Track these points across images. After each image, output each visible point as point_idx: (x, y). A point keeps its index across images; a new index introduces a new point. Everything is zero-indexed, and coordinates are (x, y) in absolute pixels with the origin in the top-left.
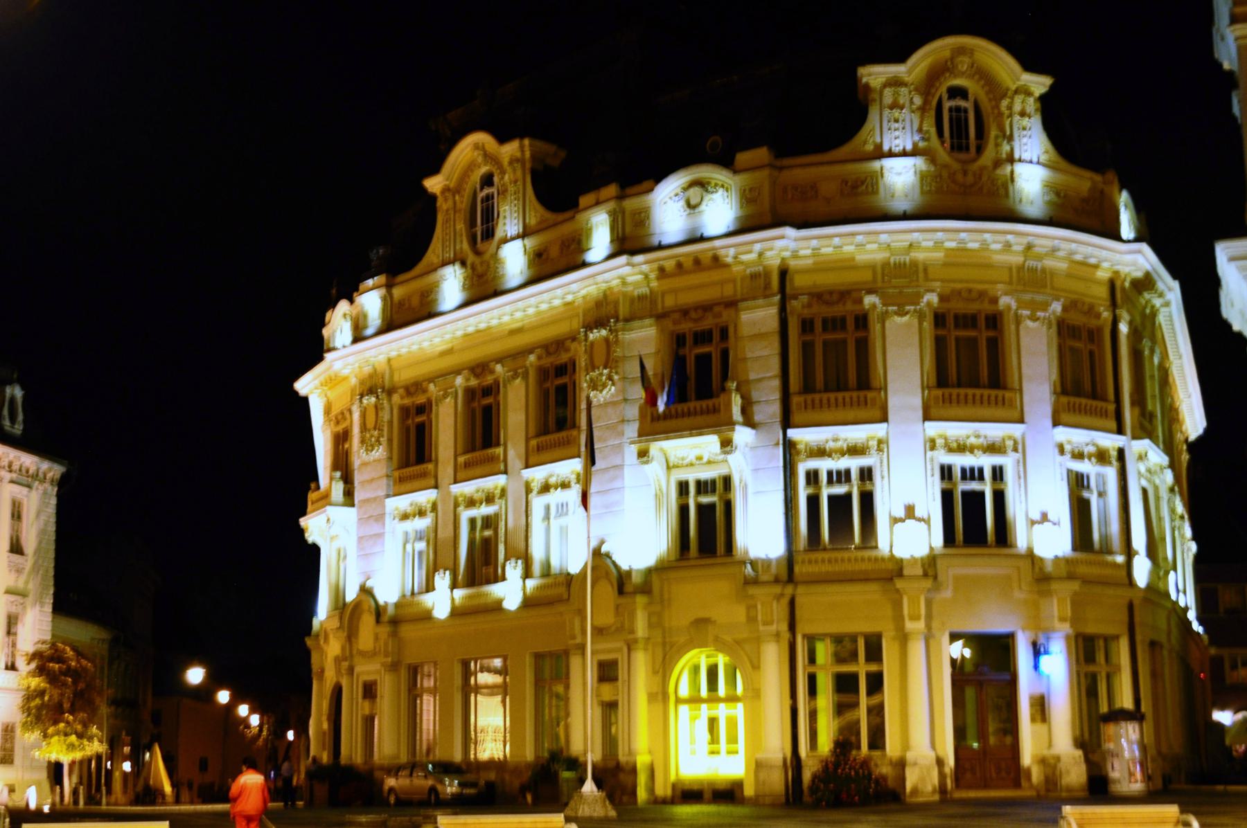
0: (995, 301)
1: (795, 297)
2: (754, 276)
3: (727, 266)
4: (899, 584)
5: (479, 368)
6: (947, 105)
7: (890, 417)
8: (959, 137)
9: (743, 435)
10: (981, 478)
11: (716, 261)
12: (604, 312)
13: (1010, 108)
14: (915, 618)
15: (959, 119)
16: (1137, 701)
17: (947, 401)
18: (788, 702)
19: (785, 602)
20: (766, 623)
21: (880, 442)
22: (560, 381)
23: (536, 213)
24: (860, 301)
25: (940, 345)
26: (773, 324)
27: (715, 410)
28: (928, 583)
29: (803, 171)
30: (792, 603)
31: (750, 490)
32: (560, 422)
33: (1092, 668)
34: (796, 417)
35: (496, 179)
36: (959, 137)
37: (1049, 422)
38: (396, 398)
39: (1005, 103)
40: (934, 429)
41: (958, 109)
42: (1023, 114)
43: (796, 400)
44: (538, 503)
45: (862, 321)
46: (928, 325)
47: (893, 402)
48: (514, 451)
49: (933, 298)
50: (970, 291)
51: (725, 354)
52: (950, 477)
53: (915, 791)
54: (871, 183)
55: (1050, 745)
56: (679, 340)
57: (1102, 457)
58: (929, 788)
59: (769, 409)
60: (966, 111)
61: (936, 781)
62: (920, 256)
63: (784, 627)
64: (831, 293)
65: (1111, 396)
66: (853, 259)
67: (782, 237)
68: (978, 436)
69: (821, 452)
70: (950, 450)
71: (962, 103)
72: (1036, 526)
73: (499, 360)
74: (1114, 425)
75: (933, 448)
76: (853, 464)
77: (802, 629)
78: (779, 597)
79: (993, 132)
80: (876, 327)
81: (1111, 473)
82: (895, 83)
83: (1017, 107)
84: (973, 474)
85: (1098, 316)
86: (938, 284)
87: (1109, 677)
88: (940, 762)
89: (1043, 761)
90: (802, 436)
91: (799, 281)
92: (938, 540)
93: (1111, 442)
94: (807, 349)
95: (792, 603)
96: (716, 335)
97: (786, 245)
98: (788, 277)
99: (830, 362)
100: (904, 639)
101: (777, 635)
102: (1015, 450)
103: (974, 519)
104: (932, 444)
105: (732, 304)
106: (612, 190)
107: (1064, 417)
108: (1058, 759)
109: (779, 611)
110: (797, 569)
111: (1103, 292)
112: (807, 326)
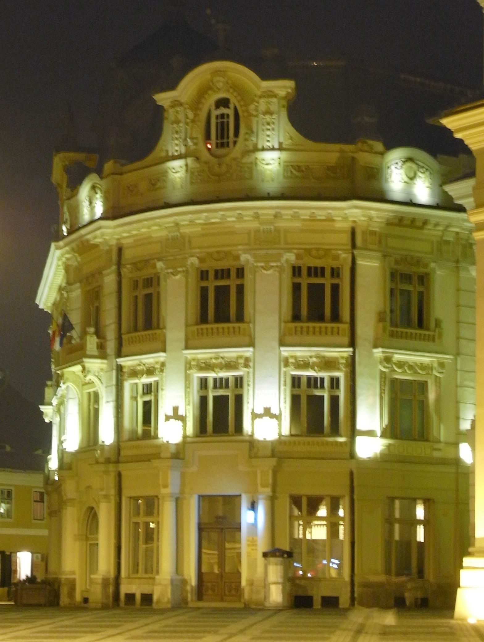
0: (237, 258)
7: (168, 348)
8: (222, 137)
17: (200, 333)
29: (135, 175)
34: (124, 350)
36: (222, 137)
37: (276, 344)
41: (222, 116)
49: (194, 261)
50: (218, 252)
53: (158, 601)
54: (158, 181)
57: (328, 364)
58: (166, 600)
60: (228, 116)
67: (100, 228)
68: (216, 358)
72: (257, 421)
74: (346, 340)
75: (190, 368)
78: (106, 472)
79: (242, 130)
80: (162, 283)
86: (197, 250)
90: (127, 362)
92: (190, 430)
93: (342, 353)
95: (119, 475)
98: (123, 251)
102: (246, 366)
103: (220, 415)
104: (188, 366)
107: (288, 339)
109: (111, 480)
111: (346, 239)
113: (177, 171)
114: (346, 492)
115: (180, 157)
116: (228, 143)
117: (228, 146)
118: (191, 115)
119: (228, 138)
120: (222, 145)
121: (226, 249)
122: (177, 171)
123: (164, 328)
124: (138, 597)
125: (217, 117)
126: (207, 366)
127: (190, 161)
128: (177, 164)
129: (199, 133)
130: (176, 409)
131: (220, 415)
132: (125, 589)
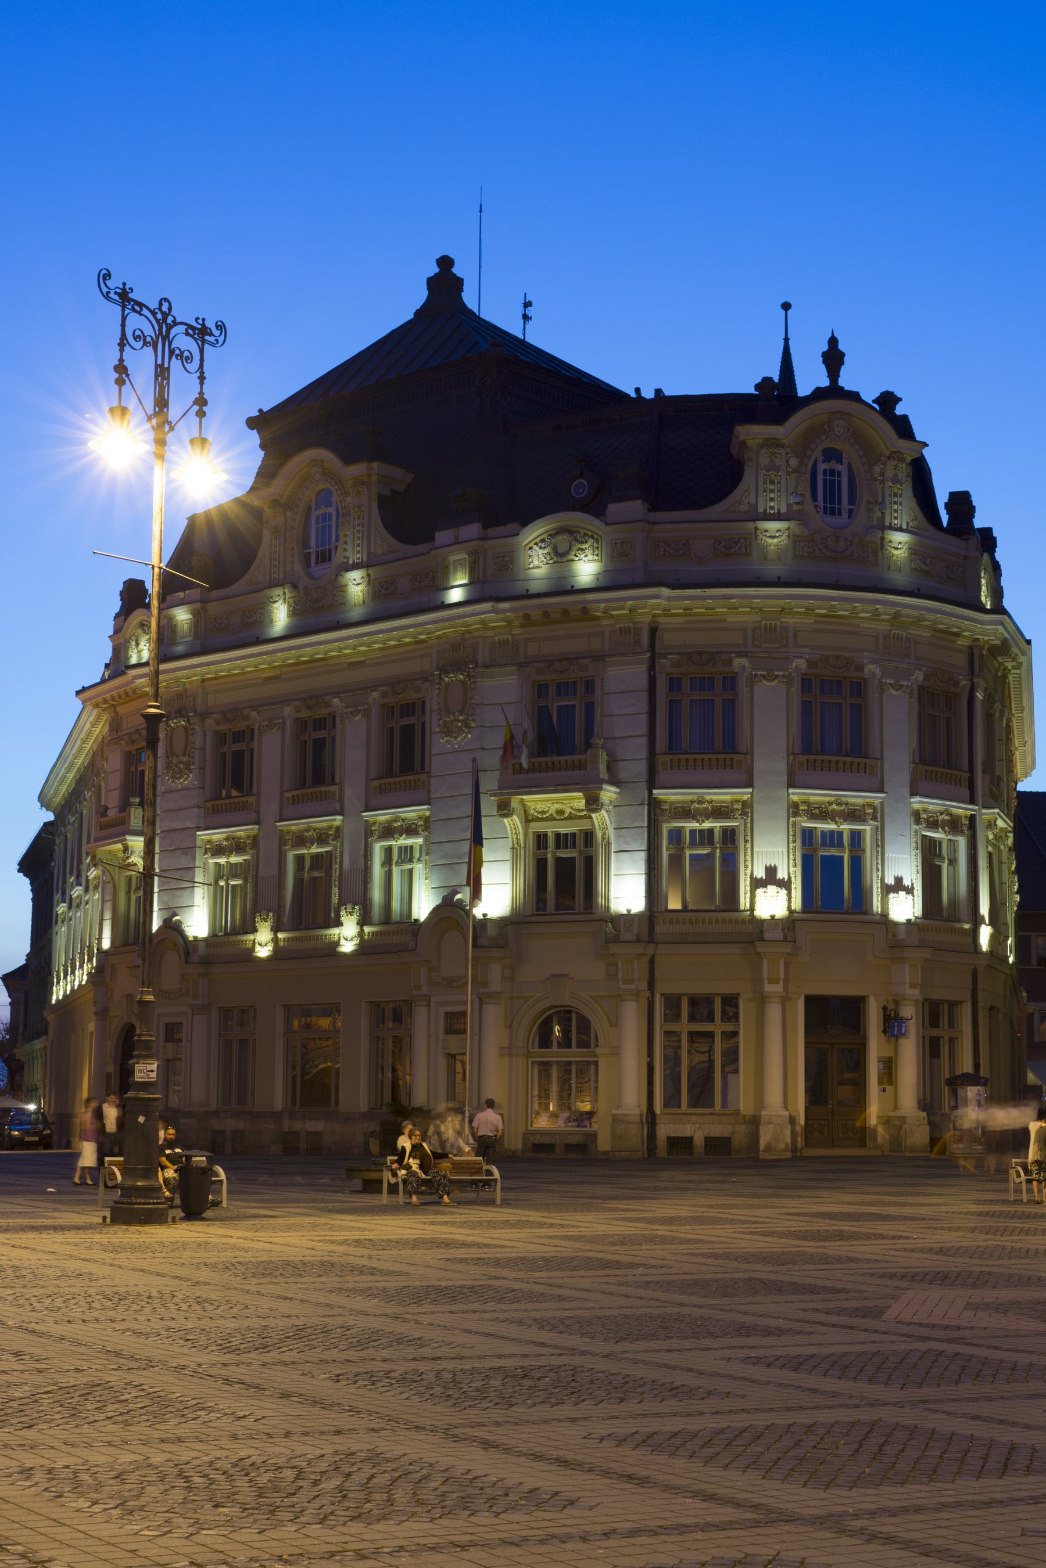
0: (860, 668)
1: (664, 655)
2: (622, 631)
3: (597, 618)
4: (761, 947)
5: (311, 700)
6: (822, 467)
7: (756, 782)
8: (832, 502)
9: (609, 793)
10: (841, 845)
11: (586, 613)
12: (460, 657)
13: (882, 474)
14: (774, 981)
15: (832, 482)
16: (977, 1066)
18: (645, 1060)
19: (647, 958)
20: (625, 982)
21: (744, 804)
22: (407, 721)
23: (383, 542)
24: (730, 663)
25: (806, 707)
26: (642, 682)
27: (581, 766)
28: (787, 948)
30: (652, 962)
31: (613, 848)
32: (404, 763)
33: (936, 1033)
34: (661, 777)
35: (334, 499)
37: (907, 791)
38: (210, 723)
39: (877, 469)
40: (796, 795)
41: (832, 472)
42: (895, 480)
43: (661, 759)
44: (378, 849)
45: (730, 682)
46: (796, 689)
47: (759, 766)
48: (352, 792)
49: (802, 664)
50: (838, 657)
51: (590, 708)
52: (811, 843)
53: (768, 1149)
54: (747, 543)
55: (895, 1108)
56: (541, 689)
58: (782, 1146)
59: (636, 767)
60: (839, 473)
61: (789, 1140)
62: (790, 620)
63: (644, 985)
64: (701, 653)
65: (966, 767)
66: (724, 621)
67: (657, 597)
68: (839, 804)
69: (685, 812)
70: (813, 817)
71: (838, 467)
73: (336, 694)
75: (796, 814)
76: (715, 825)
77: (661, 988)
81: (962, 842)
82: (773, 443)
83: (890, 474)
84: (833, 839)
85: (957, 684)
86: (807, 650)
87: (952, 1040)
88: (792, 1120)
89: (887, 1121)
91: (668, 639)
93: (961, 810)
94: (673, 707)
95: (652, 962)
96: (581, 688)
97: (658, 602)
98: (657, 634)
99: (697, 726)
100: (762, 1000)
101: (637, 994)
102: (874, 818)
103: (834, 882)
104: (794, 809)
105: (599, 657)
106: (473, 529)
108: (903, 1119)
110: (658, 929)
111: (962, 660)
112: (674, 684)
113: (774, 535)
114: (967, 995)
115: (778, 517)
116: (840, 510)
117: (840, 514)
118: (794, 462)
119: (840, 503)
120: (832, 512)
121: (847, 654)
122: (774, 535)
123: (750, 753)
124: (699, 1141)
125: (825, 471)
126: (822, 814)
127: (791, 524)
128: (773, 526)
129: (805, 487)
130: (771, 871)
131: (834, 882)
132: (665, 1130)
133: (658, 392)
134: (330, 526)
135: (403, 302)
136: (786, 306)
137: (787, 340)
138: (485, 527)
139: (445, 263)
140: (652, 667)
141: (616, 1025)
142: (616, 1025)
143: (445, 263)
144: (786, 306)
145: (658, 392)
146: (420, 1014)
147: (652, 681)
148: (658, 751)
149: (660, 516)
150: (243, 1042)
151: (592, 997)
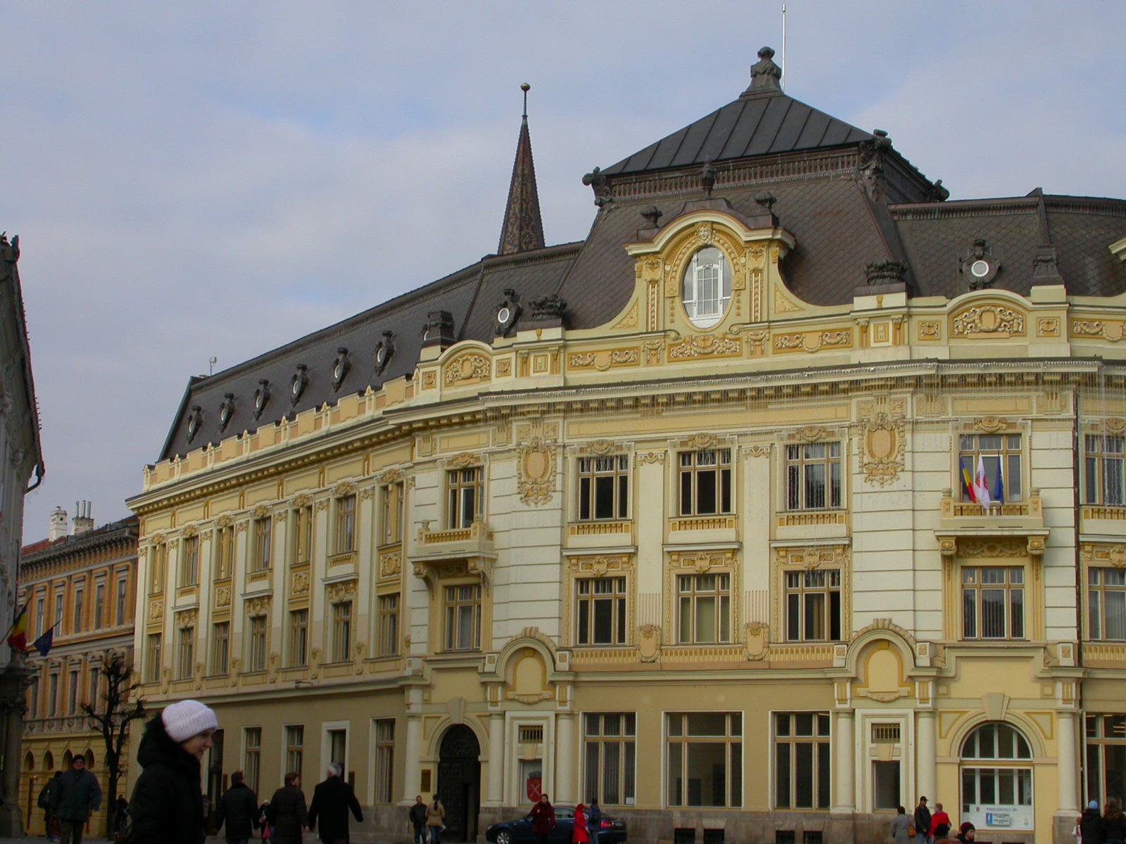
94: (1090, 462)
101: (1074, 714)
110: (1084, 655)
133: (939, 182)
134: (716, 282)
135: (735, 85)
136: (526, 88)
137: (525, 117)
138: (910, 296)
139: (767, 54)
140: (1076, 429)
141: (1052, 738)
142: (1052, 738)
143: (767, 54)
144: (526, 88)
145: (939, 182)
146: (843, 723)
147: (1076, 440)
148: (1081, 503)
149: (1078, 300)
150: (612, 749)
151: (1027, 713)
